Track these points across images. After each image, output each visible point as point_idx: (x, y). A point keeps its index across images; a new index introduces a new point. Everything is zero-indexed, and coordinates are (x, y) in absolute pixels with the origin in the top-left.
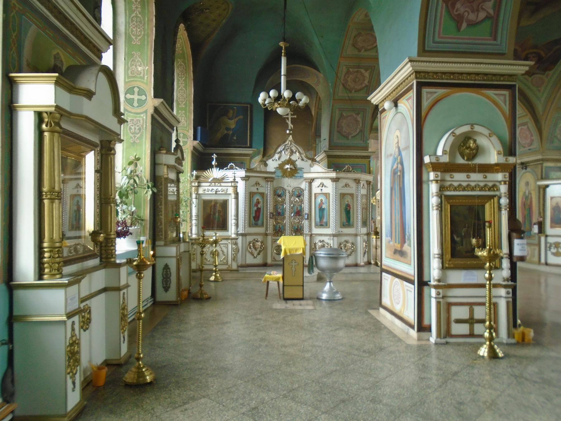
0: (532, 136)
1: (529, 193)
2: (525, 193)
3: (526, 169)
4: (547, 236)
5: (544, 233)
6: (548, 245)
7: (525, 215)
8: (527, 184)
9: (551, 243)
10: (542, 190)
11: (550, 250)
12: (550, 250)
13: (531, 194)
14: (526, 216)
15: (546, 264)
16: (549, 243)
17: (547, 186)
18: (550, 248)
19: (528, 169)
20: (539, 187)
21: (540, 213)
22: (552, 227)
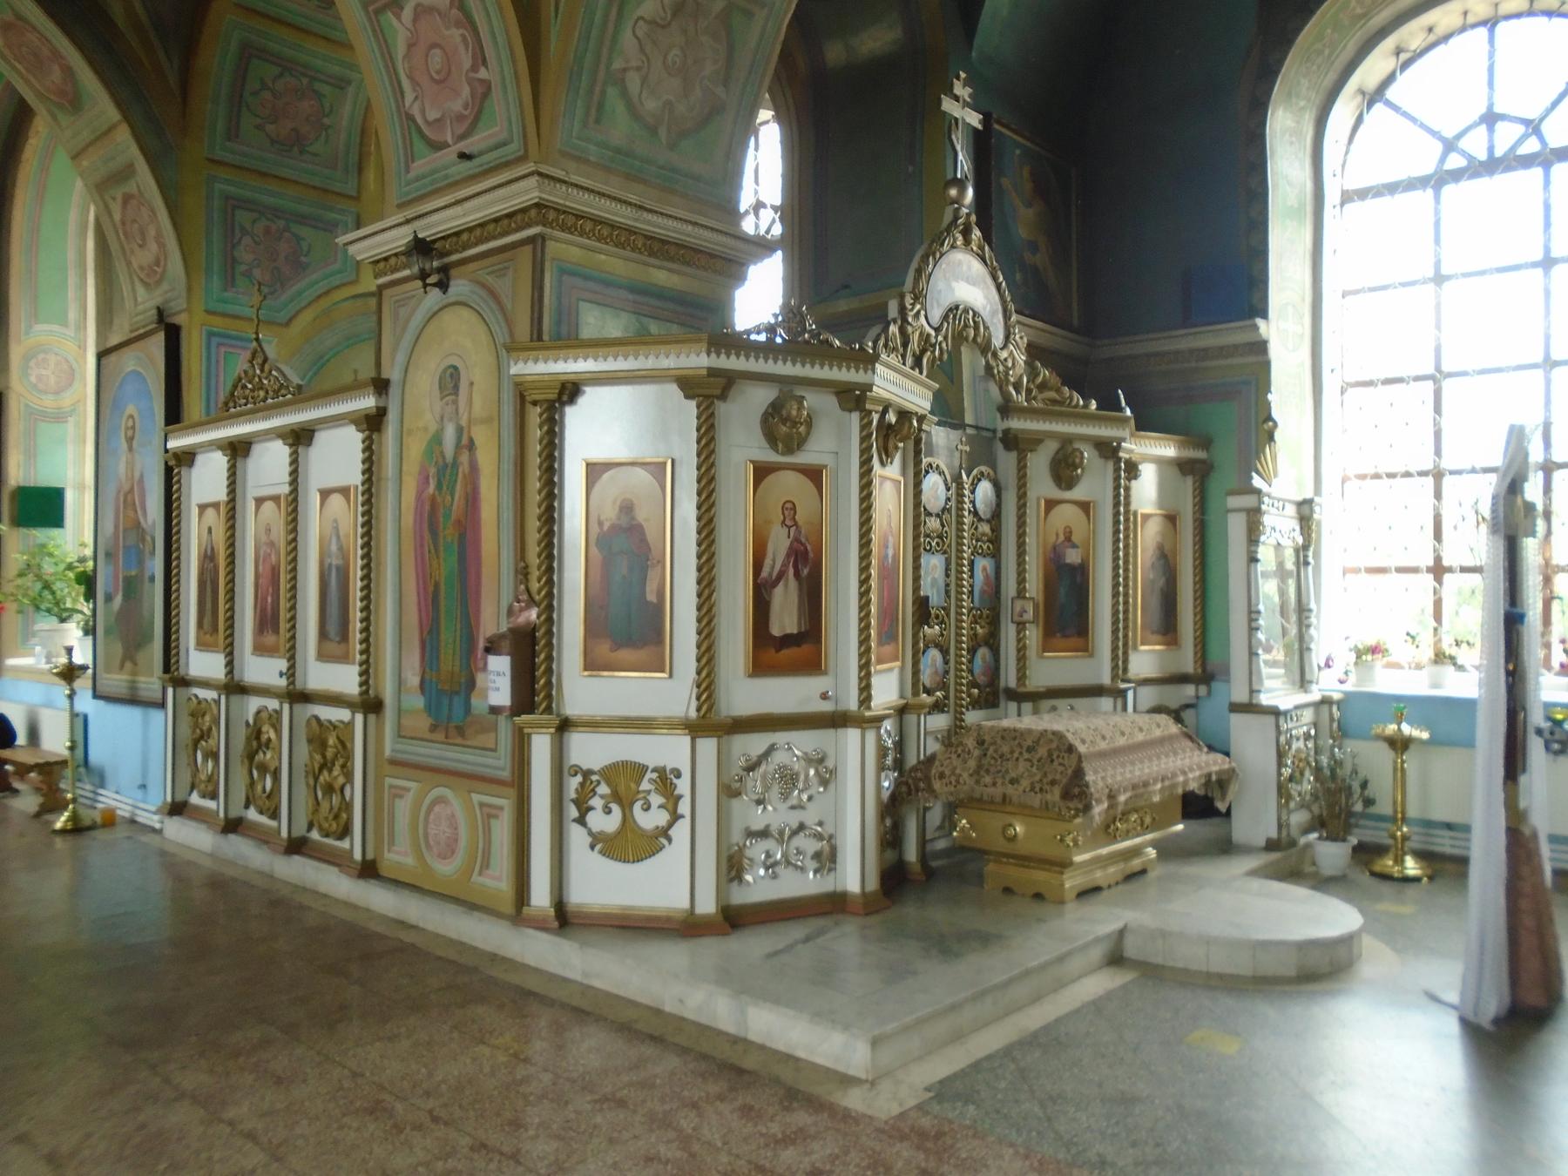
0: (481, 60)
1: (458, 446)
2: (437, 439)
3: (443, 286)
4: (565, 725)
5: (548, 710)
6: (574, 783)
7: (437, 585)
8: (451, 381)
9: (587, 774)
10: (534, 415)
11: (581, 821)
12: (581, 821)
13: (471, 446)
14: (442, 587)
15: (564, 919)
16: (576, 770)
17: (570, 391)
18: (584, 810)
19: (460, 287)
20: (523, 395)
21: (523, 573)
22: (592, 664)
